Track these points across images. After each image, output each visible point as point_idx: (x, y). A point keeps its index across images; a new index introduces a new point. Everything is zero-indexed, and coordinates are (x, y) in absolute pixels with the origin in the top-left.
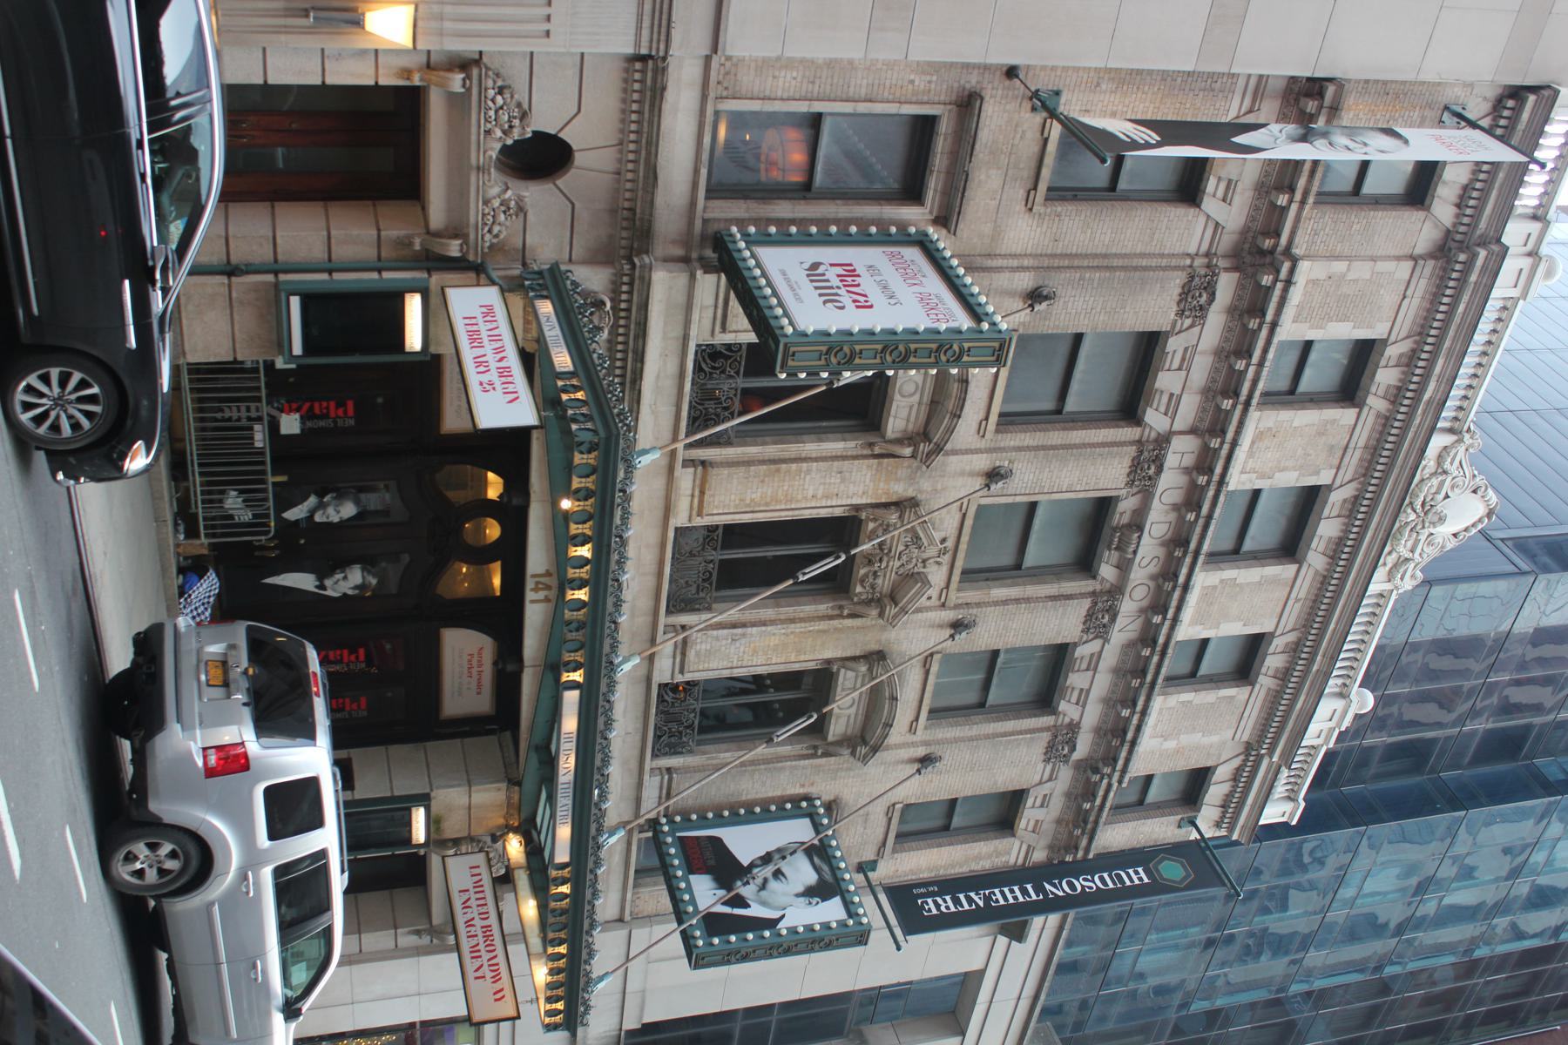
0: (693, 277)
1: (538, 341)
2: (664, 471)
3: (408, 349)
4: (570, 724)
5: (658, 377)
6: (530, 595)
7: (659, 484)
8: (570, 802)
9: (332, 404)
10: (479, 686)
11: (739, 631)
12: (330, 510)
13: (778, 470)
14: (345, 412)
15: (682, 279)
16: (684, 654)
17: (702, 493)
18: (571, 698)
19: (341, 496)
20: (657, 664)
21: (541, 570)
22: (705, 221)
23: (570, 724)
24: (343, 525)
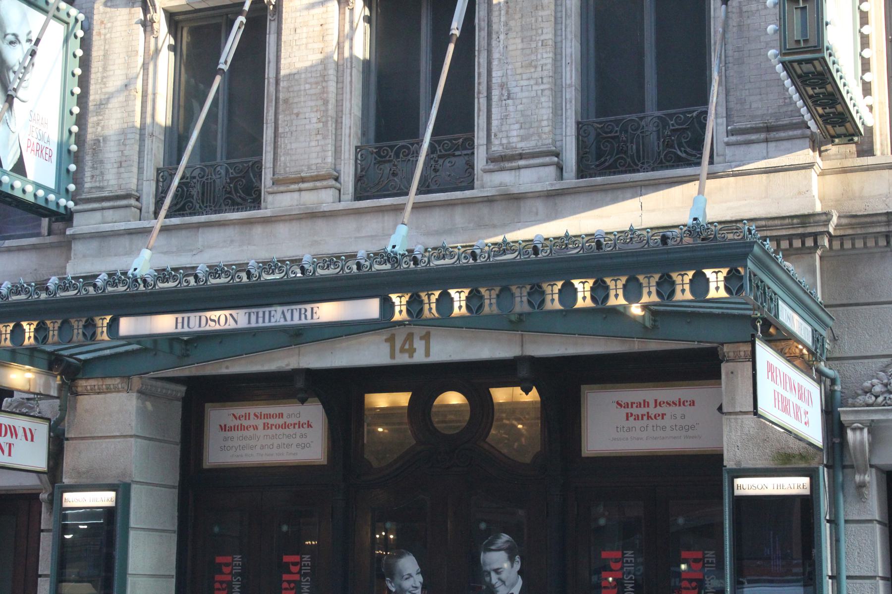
0: (74, 237)
1: (129, 377)
2: (268, 228)
3: (112, 504)
4: (164, 323)
5: (165, 253)
6: (419, 358)
7: (282, 230)
8: (279, 309)
9: (285, 577)
10: (681, 403)
11: (495, 93)
12: (407, 584)
13: (286, 101)
14: (295, 564)
15: (78, 247)
16: (521, 156)
17: (303, 180)
18: (127, 326)
19: (392, 573)
20: (523, 189)
21: (385, 348)
22: (49, 234)
23: (164, 323)
24: (424, 571)
